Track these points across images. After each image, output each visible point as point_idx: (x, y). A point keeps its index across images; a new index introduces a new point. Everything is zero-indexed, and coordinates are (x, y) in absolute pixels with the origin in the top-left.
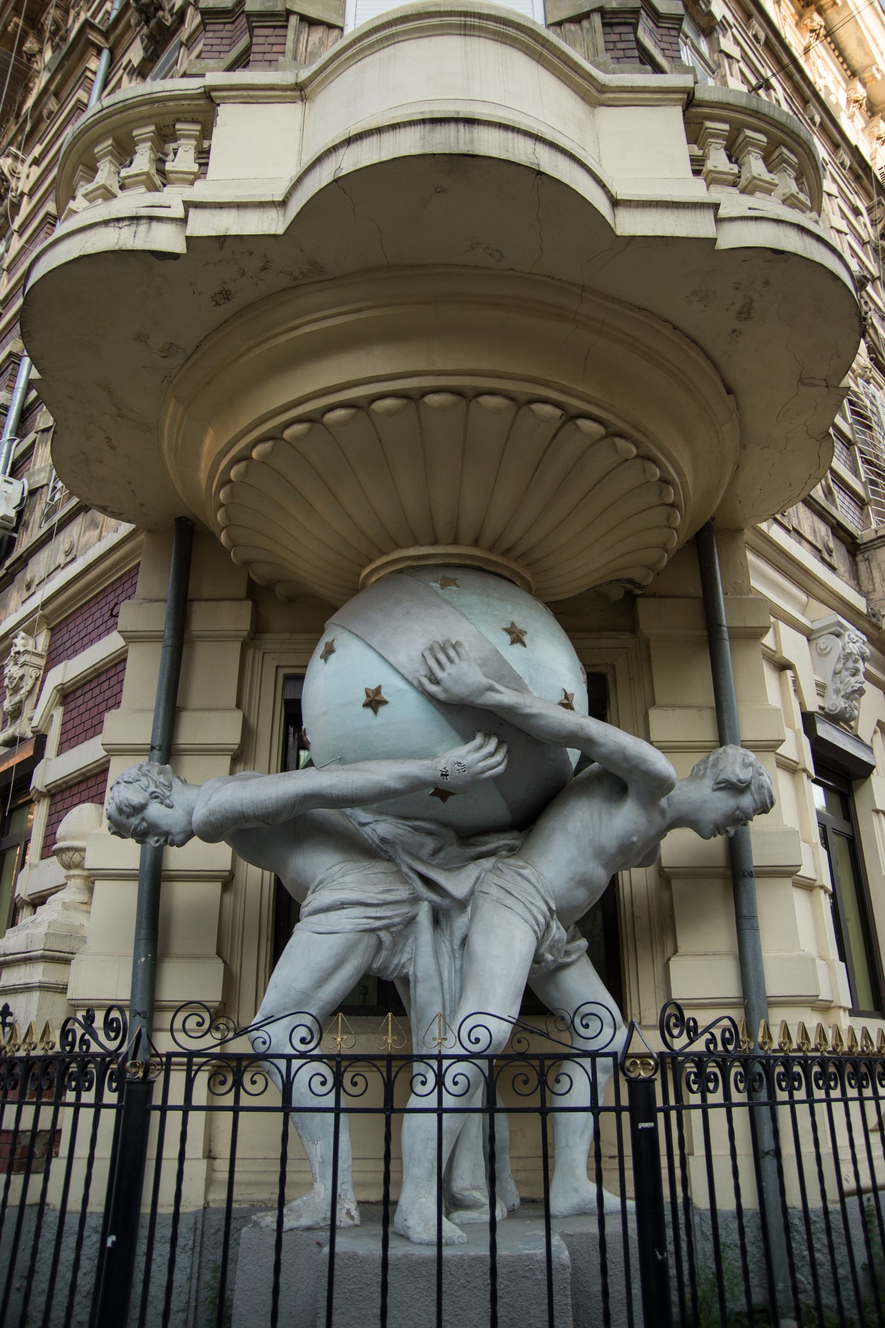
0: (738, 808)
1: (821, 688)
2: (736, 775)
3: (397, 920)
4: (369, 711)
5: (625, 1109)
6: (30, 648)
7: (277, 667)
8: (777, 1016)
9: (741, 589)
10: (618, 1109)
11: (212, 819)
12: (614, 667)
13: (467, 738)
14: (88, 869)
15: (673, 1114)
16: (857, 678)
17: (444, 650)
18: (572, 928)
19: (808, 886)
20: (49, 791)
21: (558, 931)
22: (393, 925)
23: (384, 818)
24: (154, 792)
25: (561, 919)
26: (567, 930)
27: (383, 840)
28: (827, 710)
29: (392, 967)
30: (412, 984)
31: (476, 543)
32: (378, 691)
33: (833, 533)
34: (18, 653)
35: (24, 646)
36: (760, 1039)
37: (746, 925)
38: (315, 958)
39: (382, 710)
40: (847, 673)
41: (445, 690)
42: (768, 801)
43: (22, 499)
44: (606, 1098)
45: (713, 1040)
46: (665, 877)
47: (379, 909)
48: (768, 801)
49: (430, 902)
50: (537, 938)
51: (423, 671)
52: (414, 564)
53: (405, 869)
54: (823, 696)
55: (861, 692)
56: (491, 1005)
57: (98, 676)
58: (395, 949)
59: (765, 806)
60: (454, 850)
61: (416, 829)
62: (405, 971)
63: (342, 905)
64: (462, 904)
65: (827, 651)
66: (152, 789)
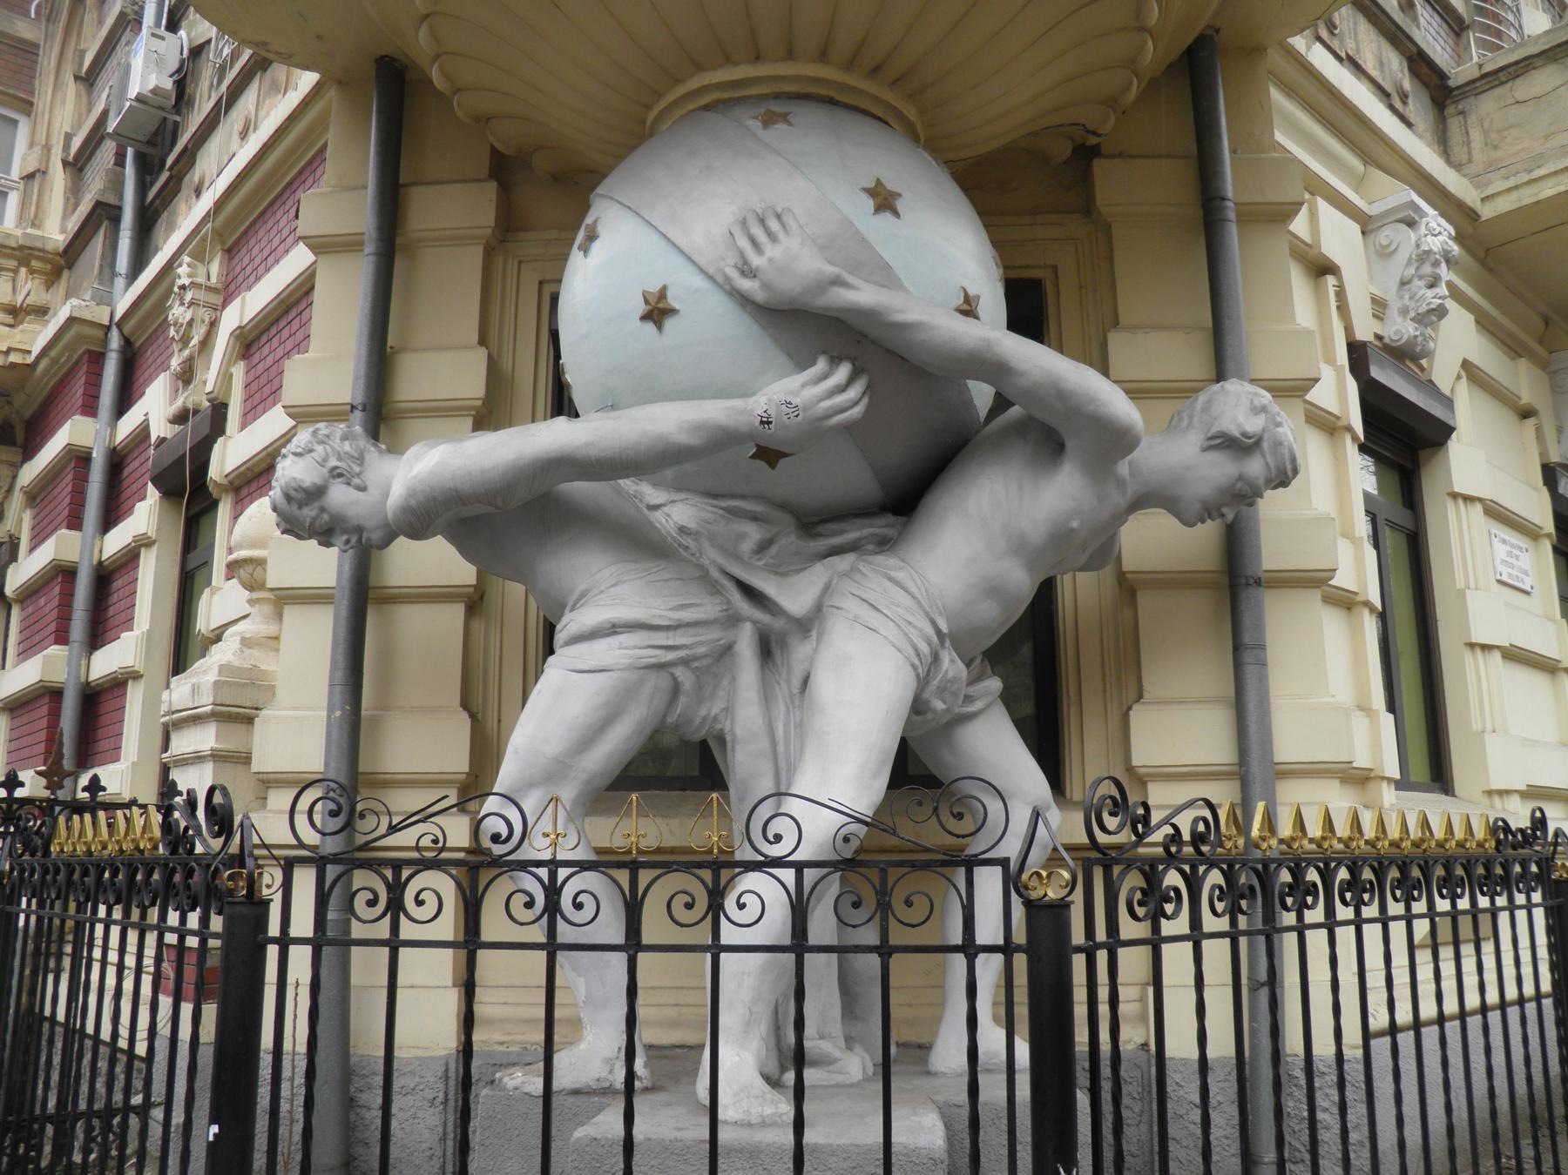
0: (1240, 478)
1: (1379, 307)
2: (1239, 426)
3: (701, 650)
4: (650, 327)
5: (1019, 949)
6: (201, 280)
7: (541, 283)
8: (1291, 795)
9: (1256, 142)
10: (1007, 949)
11: (413, 502)
12: (1055, 268)
13: (802, 364)
14: (272, 590)
15: (1102, 956)
16: (1436, 290)
17: (762, 221)
18: (977, 662)
19: (1346, 602)
20: (231, 483)
21: (952, 666)
22: (696, 658)
23: (683, 496)
24: (336, 468)
25: (957, 647)
26: (968, 666)
27: (682, 530)
28: (1386, 340)
29: (697, 721)
30: (729, 746)
31: (823, 56)
32: (662, 294)
33: (1411, 70)
34: (183, 287)
35: (189, 276)
36: (1255, 833)
37: (1248, 656)
38: (563, 712)
39: (669, 323)
40: (1422, 283)
41: (765, 286)
42: (1289, 467)
43: (182, 62)
44: (988, 930)
45: (1176, 837)
46: (1128, 588)
47: (671, 634)
48: (1289, 467)
49: (754, 622)
50: (918, 676)
51: (732, 259)
52: (725, 95)
53: (715, 573)
54: (1381, 319)
55: (1441, 312)
56: (830, 780)
57: (287, 312)
58: (700, 694)
59: (1283, 477)
60: (790, 540)
61: (729, 510)
62: (719, 726)
63: (613, 629)
64: (806, 626)
65: (1392, 248)
66: (333, 462)
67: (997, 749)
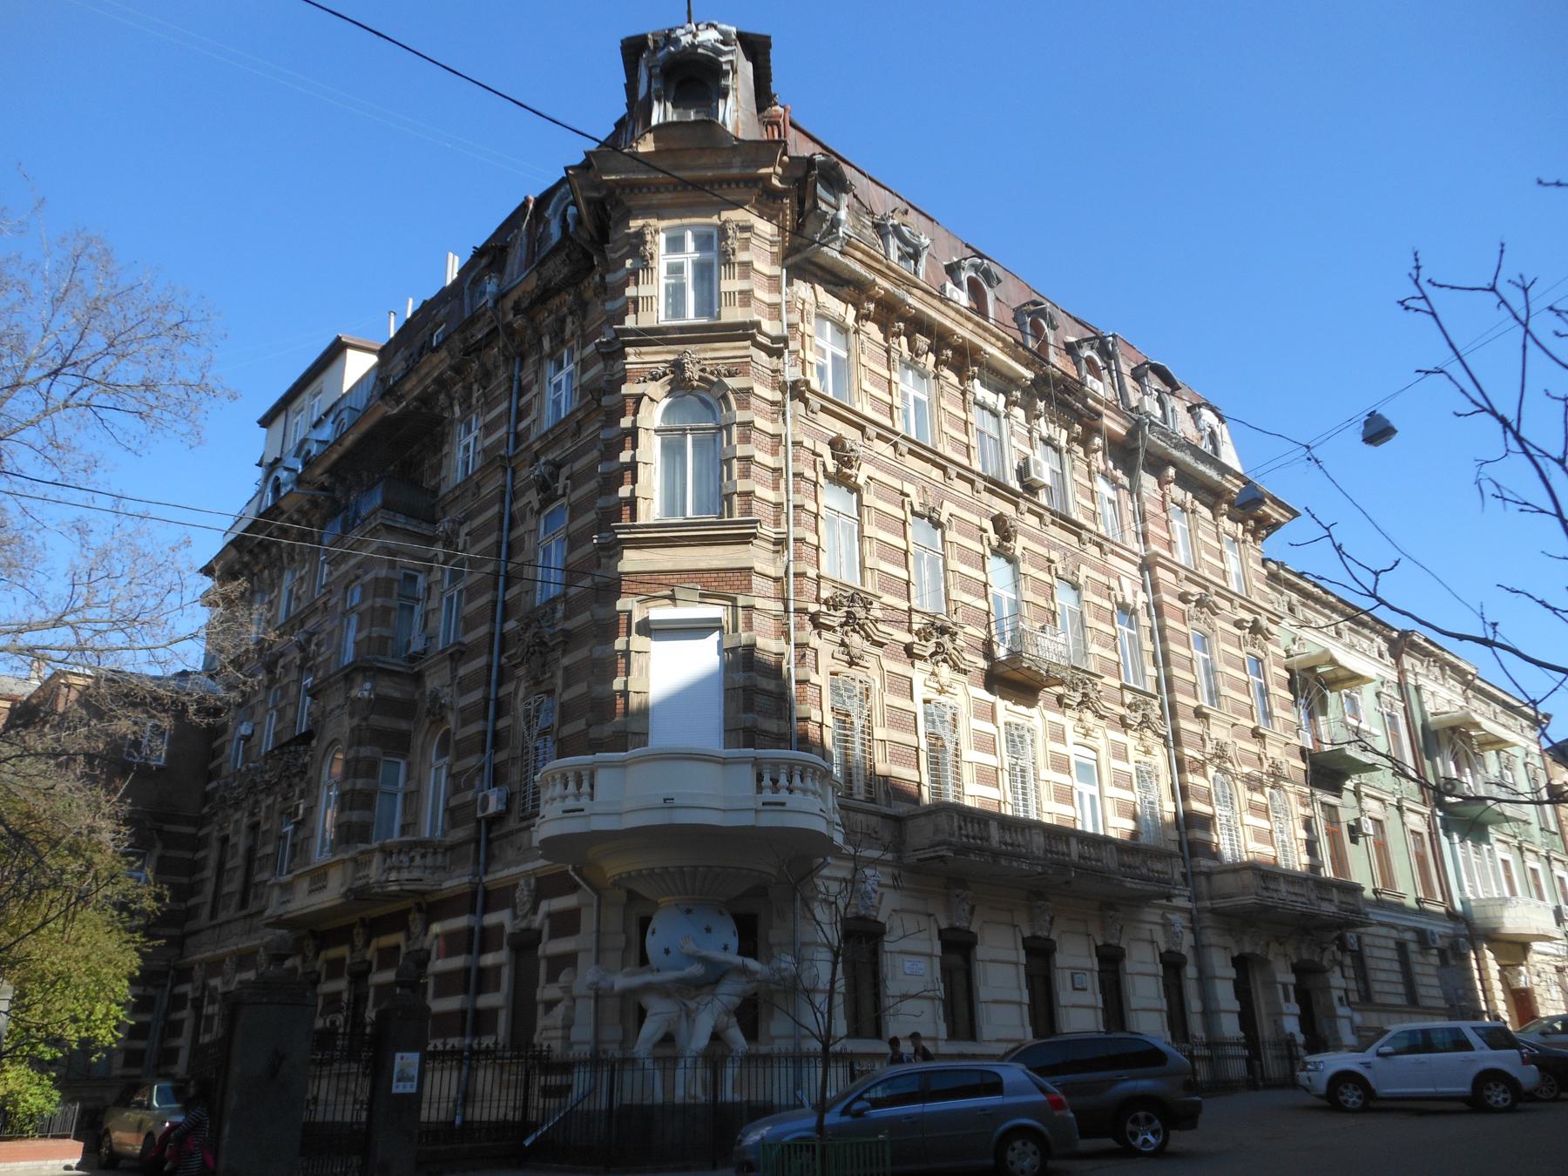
67: (736, 1036)
